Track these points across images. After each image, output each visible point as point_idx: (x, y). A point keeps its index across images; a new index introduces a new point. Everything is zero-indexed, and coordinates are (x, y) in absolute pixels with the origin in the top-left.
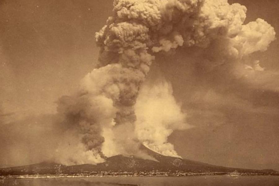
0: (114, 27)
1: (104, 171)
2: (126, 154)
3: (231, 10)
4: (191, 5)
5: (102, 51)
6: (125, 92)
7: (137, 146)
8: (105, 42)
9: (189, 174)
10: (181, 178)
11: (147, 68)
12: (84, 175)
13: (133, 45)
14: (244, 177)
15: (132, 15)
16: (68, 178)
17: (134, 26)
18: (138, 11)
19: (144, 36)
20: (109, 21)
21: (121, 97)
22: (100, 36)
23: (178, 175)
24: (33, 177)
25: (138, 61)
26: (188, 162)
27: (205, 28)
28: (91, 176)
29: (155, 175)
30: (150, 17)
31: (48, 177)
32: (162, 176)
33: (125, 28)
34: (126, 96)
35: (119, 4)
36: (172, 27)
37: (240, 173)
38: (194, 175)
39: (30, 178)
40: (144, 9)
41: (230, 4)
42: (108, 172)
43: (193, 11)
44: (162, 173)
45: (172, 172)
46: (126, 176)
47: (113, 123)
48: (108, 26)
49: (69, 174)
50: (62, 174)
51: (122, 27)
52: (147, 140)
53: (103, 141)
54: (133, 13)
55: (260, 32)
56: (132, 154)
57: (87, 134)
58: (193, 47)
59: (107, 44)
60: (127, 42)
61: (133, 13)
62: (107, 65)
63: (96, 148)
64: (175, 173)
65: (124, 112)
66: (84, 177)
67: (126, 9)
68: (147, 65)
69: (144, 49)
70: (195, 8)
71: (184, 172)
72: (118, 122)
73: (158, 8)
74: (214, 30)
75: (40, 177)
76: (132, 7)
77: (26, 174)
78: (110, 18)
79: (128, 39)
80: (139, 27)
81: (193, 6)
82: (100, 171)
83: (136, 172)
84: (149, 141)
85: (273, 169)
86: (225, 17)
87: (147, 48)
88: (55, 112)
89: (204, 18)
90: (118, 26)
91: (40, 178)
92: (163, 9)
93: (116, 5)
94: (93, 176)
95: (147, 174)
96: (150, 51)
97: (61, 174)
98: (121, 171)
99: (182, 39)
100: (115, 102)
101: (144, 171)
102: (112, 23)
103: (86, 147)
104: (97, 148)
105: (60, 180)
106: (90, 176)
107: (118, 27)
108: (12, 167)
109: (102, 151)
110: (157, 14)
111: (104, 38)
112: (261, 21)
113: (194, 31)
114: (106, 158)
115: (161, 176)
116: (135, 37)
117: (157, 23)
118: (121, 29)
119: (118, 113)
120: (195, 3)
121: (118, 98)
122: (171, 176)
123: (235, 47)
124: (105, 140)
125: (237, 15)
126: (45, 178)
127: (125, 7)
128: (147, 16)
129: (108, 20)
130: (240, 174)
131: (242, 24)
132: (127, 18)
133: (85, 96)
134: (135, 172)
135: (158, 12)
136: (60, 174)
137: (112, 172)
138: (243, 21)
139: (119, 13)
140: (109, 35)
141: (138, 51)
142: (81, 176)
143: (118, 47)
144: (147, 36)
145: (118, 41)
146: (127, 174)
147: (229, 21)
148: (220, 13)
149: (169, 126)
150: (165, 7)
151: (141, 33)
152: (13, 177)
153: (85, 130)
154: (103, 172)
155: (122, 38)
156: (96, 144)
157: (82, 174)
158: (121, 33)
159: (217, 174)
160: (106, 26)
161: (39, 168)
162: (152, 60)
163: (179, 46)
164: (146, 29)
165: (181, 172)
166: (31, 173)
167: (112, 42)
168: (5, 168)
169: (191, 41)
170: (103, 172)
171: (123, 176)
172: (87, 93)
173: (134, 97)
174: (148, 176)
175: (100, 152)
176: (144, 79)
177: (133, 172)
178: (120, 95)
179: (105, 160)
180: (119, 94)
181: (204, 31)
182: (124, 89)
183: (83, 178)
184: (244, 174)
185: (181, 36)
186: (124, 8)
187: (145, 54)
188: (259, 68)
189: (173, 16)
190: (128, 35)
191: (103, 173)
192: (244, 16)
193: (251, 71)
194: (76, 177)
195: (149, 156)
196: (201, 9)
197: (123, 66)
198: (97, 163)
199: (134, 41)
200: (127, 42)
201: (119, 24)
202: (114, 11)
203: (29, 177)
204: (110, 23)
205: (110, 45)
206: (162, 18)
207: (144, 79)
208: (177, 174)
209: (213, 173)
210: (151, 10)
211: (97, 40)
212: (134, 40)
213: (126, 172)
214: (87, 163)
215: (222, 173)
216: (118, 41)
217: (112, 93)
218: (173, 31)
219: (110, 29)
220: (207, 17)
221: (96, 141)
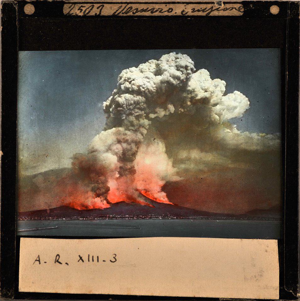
3: (213, 85)
4: (180, 80)
5: (108, 118)
11: (145, 132)
15: (133, 88)
17: (134, 97)
18: (138, 85)
21: (124, 153)
25: (137, 125)
27: (192, 99)
29: (151, 218)
33: (127, 98)
34: (128, 153)
35: (123, 79)
40: (143, 84)
41: (213, 79)
43: (182, 85)
47: (117, 175)
48: (114, 97)
51: (125, 98)
54: (133, 86)
55: (237, 102)
59: (112, 111)
60: (128, 109)
61: (133, 86)
67: (128, 83)
68: (145, 128)
69: (142, 116)
72: (121, 175)
73: (154, 82)
78: (115, 91)
81: (182, 81)
87: (145, 115)
89: (191, 91)
92: (158, 83)
93: (120, 80)
95: (145, 218)
96: (147, 117)
100: (118, 158)
110: (153, 87)
111: (110, 106)
118: (124, 99)
119: (121, 168)
121: (121, 155)
123: (216, 114)
125: (218, 88)
127: (128, 81)
129: (113, 92)
133: (95, 153)
135: (154, 86)
138: (223, 93)
139: (122, 87)
143: (121, 114)
145: (121, 109)
148: (204, 87)
150: (159, 81)
156: (103, 192)
160: (112, 97)
162: (149, 125)
164: (144, 99)
169: (180, 109)
172: (95, 151)
173: (134, 154)
176: (142, 140)
178: (123, 152)
180: (122, 151)
181: (191, 101)
186: (126, 82)
187: (143, 119)
188: (236, 131)
190: (130, 104)
191: (108, 216)
193: (230, 133)
197: (126, 130)
198: (104, 208)
200: (128, 109)
204: (115, 94)
206: (157, 90)
210: (148, 84)
211: (104, 108)
212: (134, 108)
216: (121, 109)
217: (117, 151)
219: (115, 99)
220: (194, 90)
221: (104, 190)
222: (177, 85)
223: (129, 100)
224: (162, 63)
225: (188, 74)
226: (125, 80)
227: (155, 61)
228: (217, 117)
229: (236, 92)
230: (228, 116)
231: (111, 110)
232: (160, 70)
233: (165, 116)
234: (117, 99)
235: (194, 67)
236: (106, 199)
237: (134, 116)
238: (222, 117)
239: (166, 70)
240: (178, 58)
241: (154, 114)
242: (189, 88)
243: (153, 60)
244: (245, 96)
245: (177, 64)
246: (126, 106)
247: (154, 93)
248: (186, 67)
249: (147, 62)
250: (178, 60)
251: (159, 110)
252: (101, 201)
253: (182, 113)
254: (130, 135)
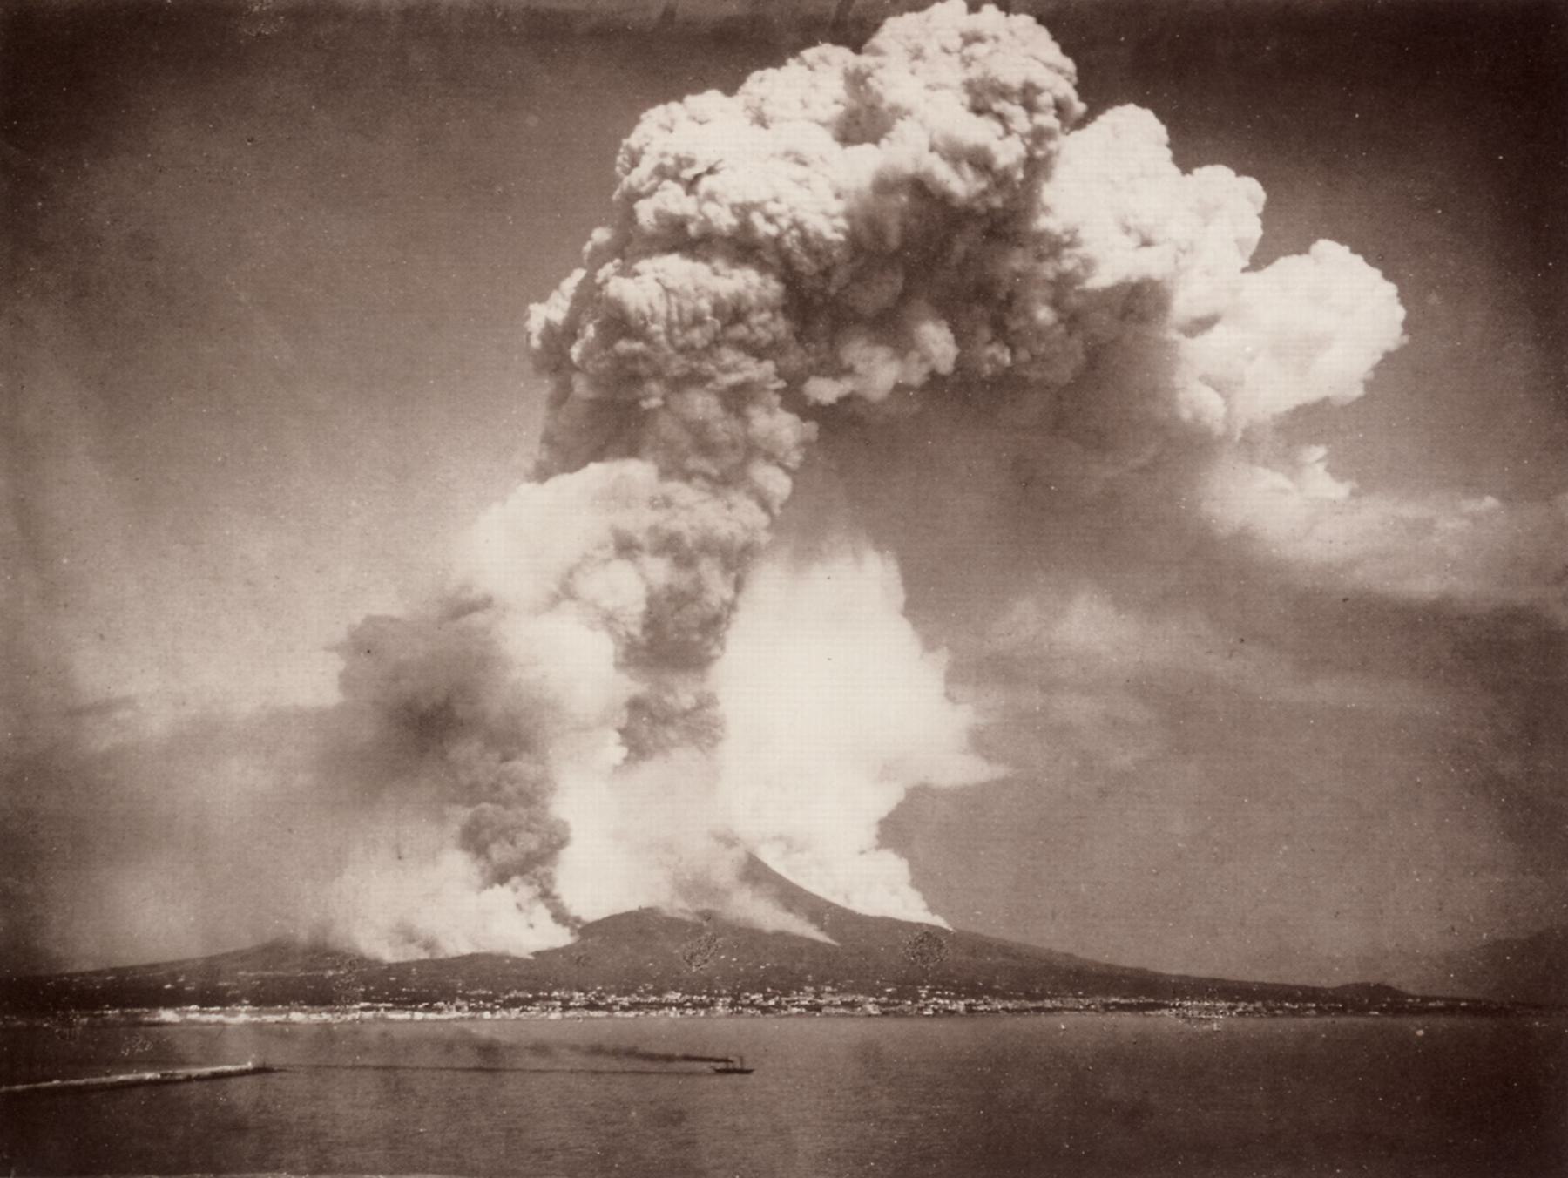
0: (621, 280)
1: (570, 989)
2: (677, 906)
4: (994, 175)
5: (561, 398)
6: (669, 599)
7: (724, 871)
9: (981, 1008)
10: (941, 1025)
11: (777, 483)
12: (471, 1009)
13: (709, 367)
14: (1251, 1022)
15: (707, 221)
16: (392, 1021)
17: (716, 273)
18: (739, 200)
19: (768, 326)
20: (597, 250)
21: (653, 622)
22: (549, 327)
23: (929, 1012)
24: (220, 1017)
25: (734, 446)
26: (978, 946)
27: (1064, 283)
28: (504, 1013)
29: (818, 1008)
30: (795, 232)
31: (296, 1016)
32: (852, 1016)
33: (670, 283)
36: (899, 281)
37: (1232, 1004)
38: (1006, 1009)
39: (208, 1024)
42: (586, 993)
43: (1005, 202)
44: (849, 999)
45: (901, 995)
46: (674, 1013)
48: (591, 276)
49: (400, 1005)
50: (363, 1004)
51: (658, 280)
53: (563, 843)
56: (706, 905)
57: (485, 805)
58: (1008, 383)
59: (582, 361)
60: (682, 350)
61: (710, 209)
62: (584, 464)
63: (528, 877)
64: (916, 999)
65: (669, 699)
66: (471, 1019)
68: (780, 465)
69: (765, 390)
70: (1014, 190)
71: (957, 998)
72: (638, 748)
74: (1105, 297)
75: (255, 1019)
76: (706, 184)
77: (189, 1004)
78: (601, 235)
79: (688, 336)
80: (744, 282)
81: (1002, 180)
82: (550, 992)
83: (726, 996)
84: (789, 844)
85: (1393, 982)
86: (1155, 236)
87: (781, 384)
88: (331, 696)
89: (1058, 237)
90: (637, 274)
91: (255, 1024)
92: (858, 193)
93: (628, 172)
94: (515, 1012)
95: (778, 1005)
96: (793, 399)
97: (357, 1002)
98: (651, 987)
99: (951, 337)
100: (621, 649)
101: (763, 992)
102: (611, 260)
103: (483, 872)
104: (535, 876)
105: (355, 1030)
106: (498, 1016)
107: (637, 279)
108: (119, 965)
109: (555, 892)
111: (570, 331)
112: (1327, 249)
113: (1011, 297)
114: (579, 926)
115: (844, 1015)
117: (828, 262)
118: (655, 291)
120: (1015, 167)
121: (636, 631)
122: (896, 1015)
123: (1206, 380)
124: (573, 834)
126: (277, 1022)
127: (676, 178)
128: (780, 227)
129: (588, 247)
130: (1231, 1009)
131: (1244, 270)
132: (686, 233)
133: (478, 619)
134: (720, 995)
136: (351, 1004)
137: (609, 993)
139: (645, 212)
140: (595, 318)
142: (455, 1014)
143: (636, 379)
144: (782, 326)
145: (638, 346)
146: (680, 1006)
147: (1181, 255)
148: (1136, 217)
149: (886, 772)
151: (750, 309)
152: (122, 1014)
153: (472, 786)
154: (564, 994)
155: (658, 333)
156: (528, 854)
157: (459, 1002)
158: (651, 306)
159: (1120, 1007)
160: (579, 274)
161: (252, 974)
163: (934, 377)
165: (941, 997)
166: (211, 997)
167: (610, 352)
168: (83, 974)
169: (993, 350)
170: (564, 994)
171: (661, 1012)
172: (486, 603)
173: (714, 624)
174: (783, 1012)
175: (546, 896)
176: (764, 538)
177: (709, 995)
178: (649, 613)
179: (572, 934)
180: (642, 607)
181: (1055, 304)
182: (670, 587)
183: (466, 1025)
184: (1251, 1008)
185: (944, 323)
186: (668, 183)
187: (770, 411)
189: (904, 225)
190: (687, 317)
191: (562, 1000)
194: (432, 1016)
195: (791, 916)
196: (1040, 191)
197: (665, 474)
198: (533, 950)
199: (714, 348)
200: (682, 350)
201: (643, 265)
202: (618, 202)
203: (205, 1018)
205: (602, 365)
206: (853, 239)
207: (764, 538)
208: (921, 1003)
209: (1098, 999)
211: (536, 343)
212: (716, 342)
213: (674, 996)
214: (485, 947)
215: (1143, 1000)
216: (638, 346)
217: (608, 603)
218: (904, 297)
219: (599, 288)
220: (1074, 232)
221: (530, 842)
222: (971, 199)
223: (688, 296)
232: (872, 107)
233: (899, 389)
242: (1044, 223)
245: (975, 72)
247: (835, 253)
251: (867, 352)
252: (519, 906)
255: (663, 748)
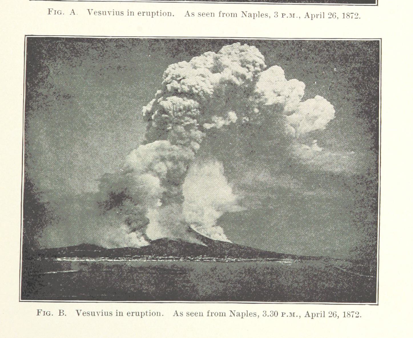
0: (163, 101)
8: (153, 117)
11: (197, 146)
12: (127, 259)
17: (184, 100)
19: (196, 112)
21: (168, 175)
28: (133, 260)
31: (87, 260)
46: (171, 260)
47: (159, 204)
48: (157, 101)
49: (110, 258)
51: (171, 102)
52: (195, 223)
53: (148, 223)
54: (183, 86)
60: (176, 117)
61: (183, 86)
78: (159, 92)
81: (248, 81)
86: (281, 94)
93: (165, 78)
94: (136, 260)
95: (194, 259)
96: (201, 128)
116: (186, 112)
119: (164, 193)
123: (291, 125)
125: (295, 92)
127: (176, 80)
129: (156, 94)
134: (181, 257)
139: (169, 87)
141: (188, 128)
143: (166, 123)
145: (166, 116)
146: (172, 259)
160: (154, 100)
163: (232, 123)
164: (197, 104)
172: (132, 171)
173: (183, 176)
181: (259, 108)
186: (174, 81)
190: (177, 110)
192: (302, 93)
197: (172, 144)
204: (159, 96)
207: (194, 158)
208: (226, 259)
211: (144, 115)
219: (158, 103)
221: (140, 223)
224: (221, 57)
225: (256, 72)
226: (172, 78)
227: (212, 54)
228: (293, 130)
229: (318, 97)
230: (306, 128)
231: (153, 117)
233: (224, 125)
234: (161, 104)
235: (264, 63)
236: (144, 235)
237: (184, 126)
238: (298, 129)
239: (228, 67)
240: (244, 51)
241: (210, 123)
242: (256, 90)
243: (209, 52)
244: (329, 103)
245: (242, 58)
246: (173, 113)
248: (254, 63)
249: (202, 55)
250: (243, 53)
251: (217, 118)
253: (247, 124)
254: (177, 151)
255: (170, 203)
